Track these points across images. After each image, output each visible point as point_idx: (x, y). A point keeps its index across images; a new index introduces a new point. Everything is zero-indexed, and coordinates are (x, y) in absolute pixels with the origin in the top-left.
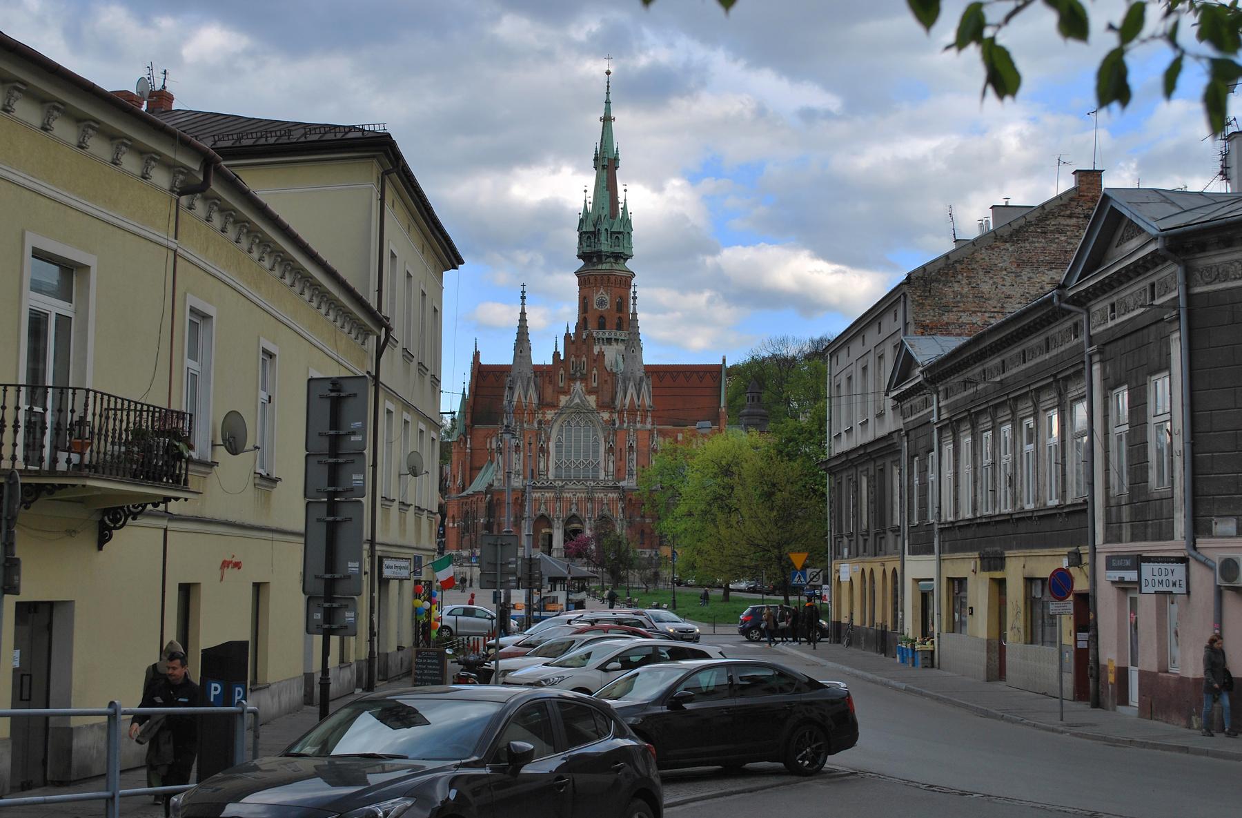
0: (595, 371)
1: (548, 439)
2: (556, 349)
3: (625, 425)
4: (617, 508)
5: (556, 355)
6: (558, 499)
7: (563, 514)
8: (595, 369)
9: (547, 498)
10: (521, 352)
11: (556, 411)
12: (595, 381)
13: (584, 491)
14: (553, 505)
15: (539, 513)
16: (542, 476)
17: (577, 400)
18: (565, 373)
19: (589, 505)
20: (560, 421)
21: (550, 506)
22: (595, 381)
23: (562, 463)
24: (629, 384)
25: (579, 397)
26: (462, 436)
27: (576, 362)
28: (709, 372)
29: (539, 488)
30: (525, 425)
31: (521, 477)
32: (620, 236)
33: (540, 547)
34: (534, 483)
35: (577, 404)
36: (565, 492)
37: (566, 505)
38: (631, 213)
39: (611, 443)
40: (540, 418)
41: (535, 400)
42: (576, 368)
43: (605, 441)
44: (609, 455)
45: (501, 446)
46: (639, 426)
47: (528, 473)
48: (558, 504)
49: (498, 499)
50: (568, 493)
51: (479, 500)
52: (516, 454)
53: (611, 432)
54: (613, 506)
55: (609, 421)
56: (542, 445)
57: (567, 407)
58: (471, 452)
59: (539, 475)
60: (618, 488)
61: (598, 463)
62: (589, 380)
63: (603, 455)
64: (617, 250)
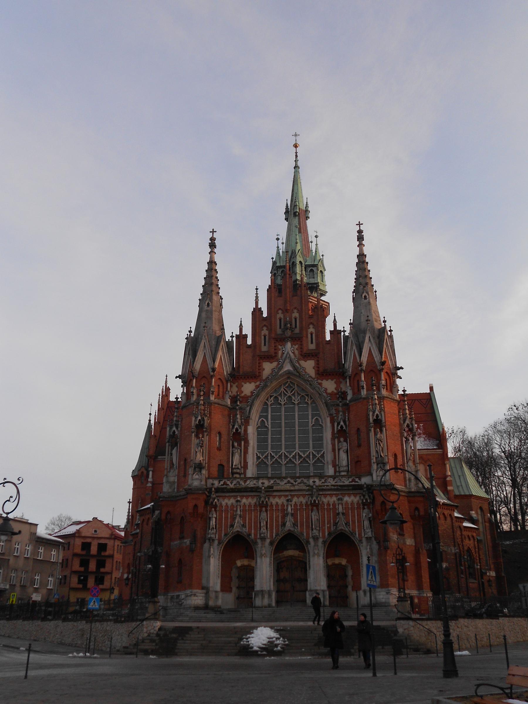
0: (311, 330)
1: (246, 421)
2: (257, 303)
3: (364, 393)
4: (359, 521)
5: (257, 312)
6: (263, 506)
7: (272, 533)
8: (311, 326)
9: (245, 505)
10: (208, 304)
11: (258, 383)
12: (312, 343)
13: (304, 493)
14: (256, 517)
15: (232, 532)
16: (238, 476)
17: (288, 367)
18: (269, 334)
19: (314, 516)
20: (263, 396)
21: (250, 519)
22: (312, 343)
23: (266, 457)
24: (364, 338)
25: (291, 362)
26: (143, 470)
27: (285, 318)
28: (417, 400)
29: (232, 490)
30: (212, 398)
31: (204, 472)
32: (315, 269)
33: (234, 589)
34: (225, 483)
35: (289, 373)
36: (274, 497)
37: (277, 517)
38: (323, 256)
39: (342, 423)
40: (234, 393)
41: (226, 370)
42: (285, 325)
43: (332, 422)
44: (339, 442)
45: (176, 433)
46: (384, 392)
47: (215, 470)
48: (264, 514)
49: (168, 512)
50: (280, 497)
51: (145, 523)
52: (197, 436)
53: (340, 409)
54: (353, 516)
55: (336, 394)
56: (237, 430)
57: (274, 374)
58: (152, 486)
59: (233, 473)
60: (360, 487)
61: (322, 456)
62: (304, 338)
63: (329, 442)
64: (312, 281)
